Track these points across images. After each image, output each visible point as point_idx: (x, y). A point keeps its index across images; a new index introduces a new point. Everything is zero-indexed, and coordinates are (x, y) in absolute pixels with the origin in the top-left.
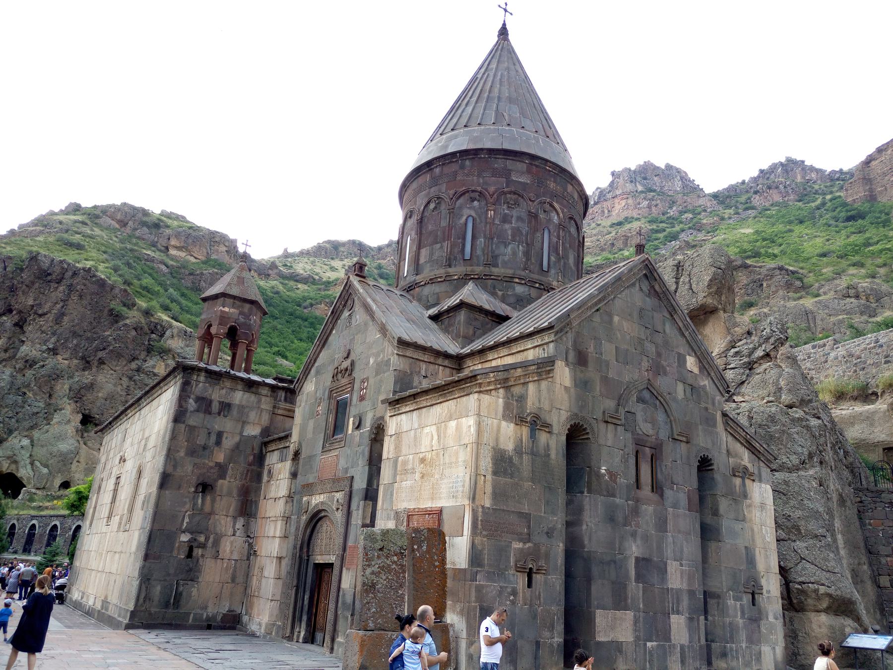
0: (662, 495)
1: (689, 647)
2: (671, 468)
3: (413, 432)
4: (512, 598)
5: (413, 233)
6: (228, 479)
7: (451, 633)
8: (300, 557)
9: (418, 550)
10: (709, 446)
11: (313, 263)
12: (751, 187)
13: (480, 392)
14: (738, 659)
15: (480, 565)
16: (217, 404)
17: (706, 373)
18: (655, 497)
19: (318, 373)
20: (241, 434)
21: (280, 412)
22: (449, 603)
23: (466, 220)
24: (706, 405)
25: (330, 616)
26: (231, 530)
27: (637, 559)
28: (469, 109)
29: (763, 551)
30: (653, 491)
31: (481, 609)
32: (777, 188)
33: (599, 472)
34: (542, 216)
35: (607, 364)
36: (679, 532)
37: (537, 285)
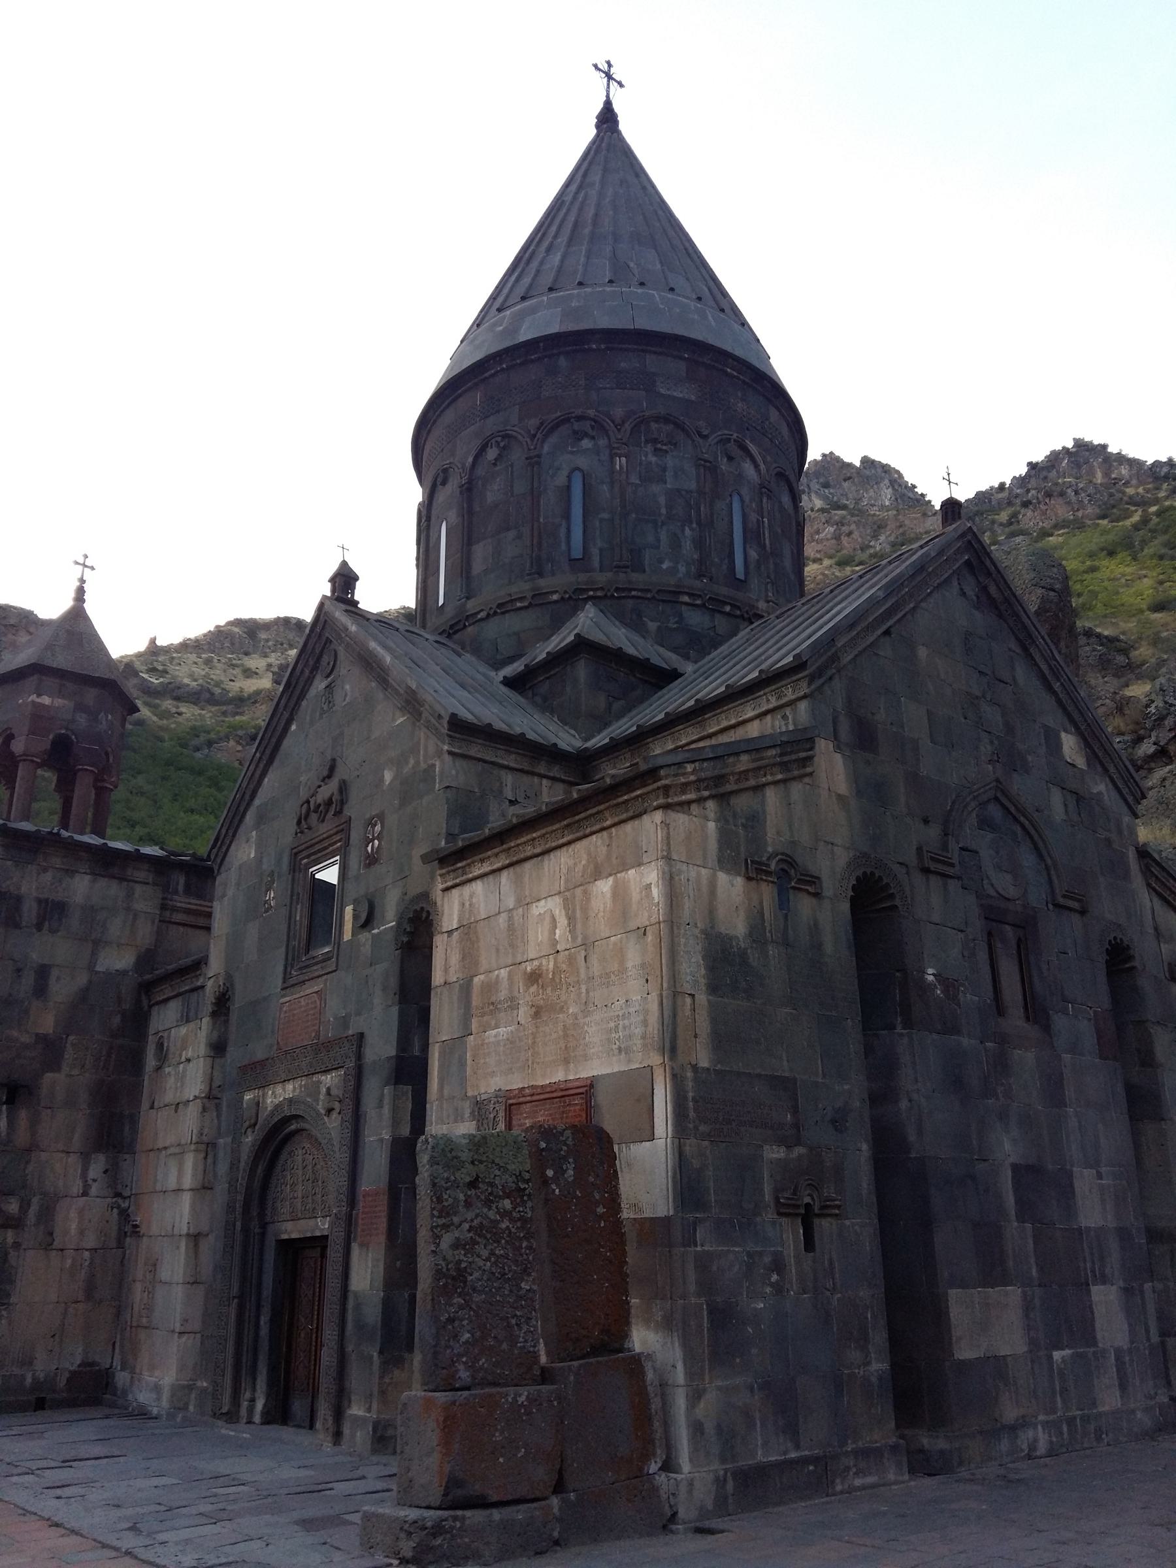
0: (1047, 1028)
3: (504, 916)
4: (775, 1277)
5: (453, 515)
6: (65, 1069)
7: (650, 1376)
8: (246, 1230)
9: (556, 1179)
11: (208, 662)
12: (1017, 496)
13: (666, 807)
16: (35, 905)
17: (1100, 769)
19: (261, 819)
20: (91, 967)
21: (179, 917)
22: (634, 1301)
23: (569, 477)
25: (328, 1357)
26: (79, 1183)
27: (1015, 1168)
28: (556, 258)
30: (1028, 1019)
32: (1062, 494)
33: (923, 980)
34: (724, 465)
37: (728, 608)
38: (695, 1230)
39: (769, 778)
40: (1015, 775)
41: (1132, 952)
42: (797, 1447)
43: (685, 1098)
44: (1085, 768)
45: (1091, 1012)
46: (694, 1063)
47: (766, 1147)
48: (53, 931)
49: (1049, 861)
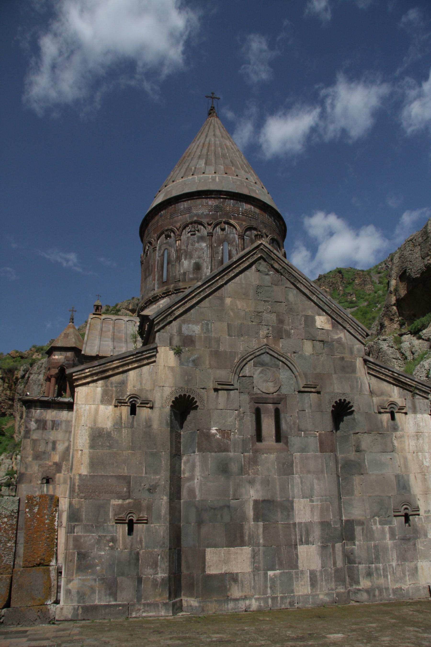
0: (287, 443)
1: (321, 572)
2: (298, 418)
4: (111, 544)
6: (63, 472)
10: (347, 390)
14: (386, 576)
15: (76, 520)
17: (340, 327)
18: (281, 445)
23: (164, 252)
24: (343, 355)
27: (256, 502)
29: (419, 476)
31: (78, 554)
35: (218, 341)
36: (309, 472)
38: (74, 528)
39: (130, 367)
40: (281, 340)
41: (351, 405)
42: (116, 600)
43: (74, 485)
44: (331, 329)
45: (318, 434)
46: (80, 473)
47: (112, 500)
48: (56, 430)
49: (297, 373)
